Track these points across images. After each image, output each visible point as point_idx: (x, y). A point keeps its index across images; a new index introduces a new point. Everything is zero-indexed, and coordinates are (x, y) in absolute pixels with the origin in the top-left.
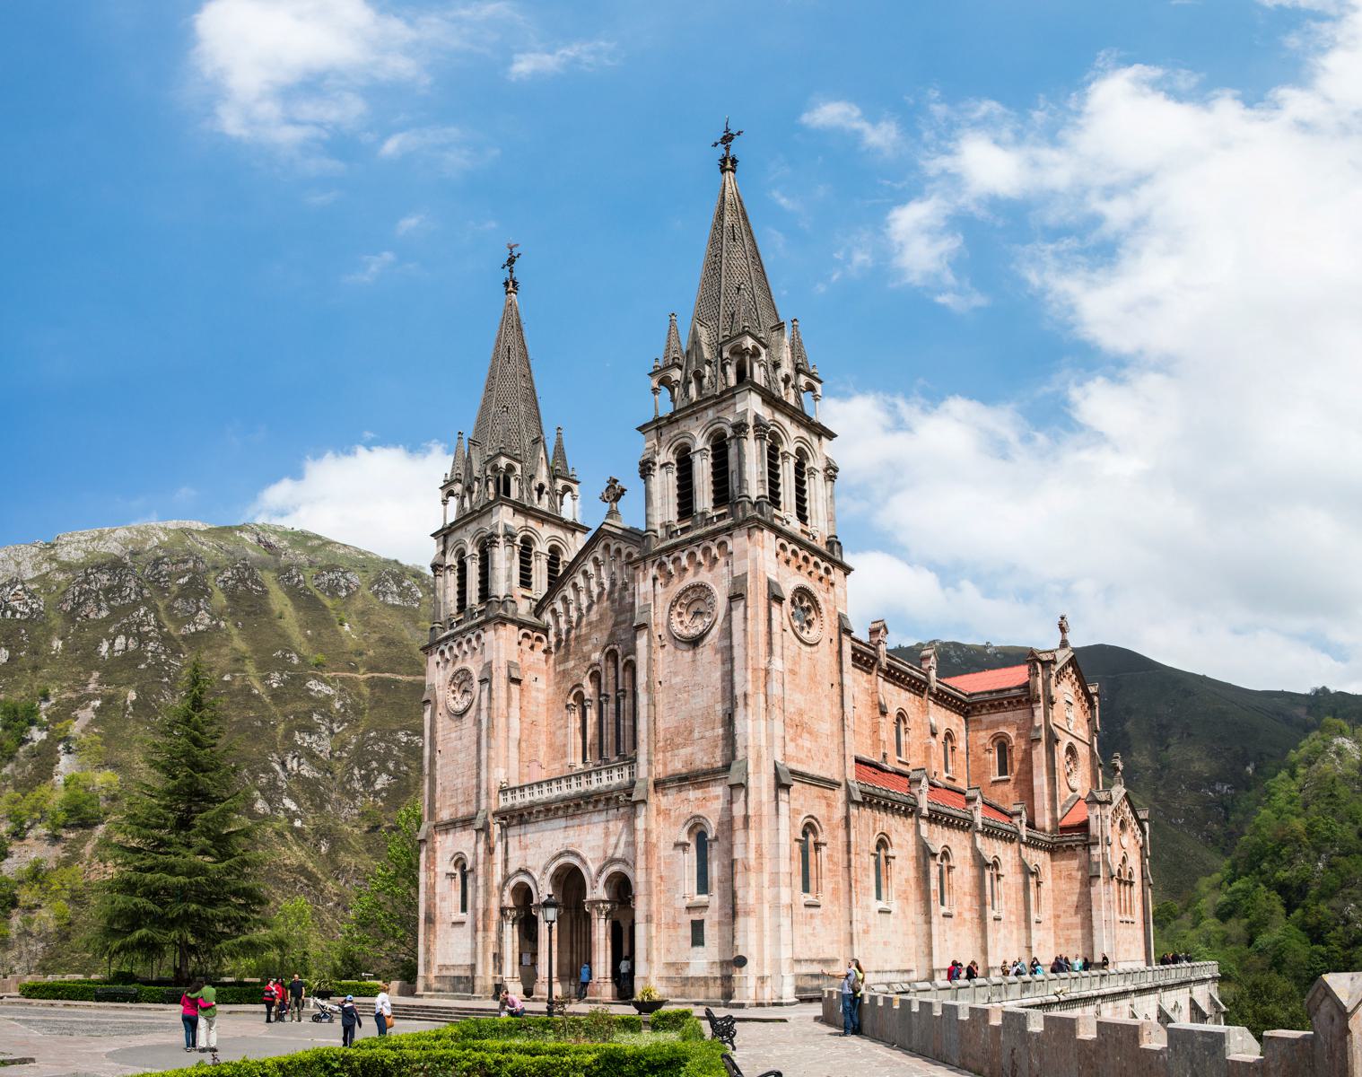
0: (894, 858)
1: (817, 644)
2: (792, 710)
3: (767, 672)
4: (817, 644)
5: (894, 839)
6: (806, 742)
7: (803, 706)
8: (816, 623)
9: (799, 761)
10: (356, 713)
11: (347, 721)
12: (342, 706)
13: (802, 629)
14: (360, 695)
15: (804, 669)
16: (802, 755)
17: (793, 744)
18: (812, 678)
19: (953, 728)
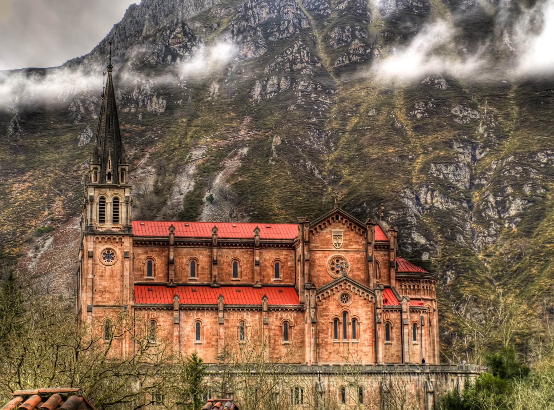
0: (160, 326)
1: (114, 264)
2: (100, 287)
3: (87, 279)
4: (114, 264)
5: (161, 319)
6: (107, 296)
7: (106, 285)
8: (115, 258)
9: (104, 302)
10: (499, 138)
11: (489, 146)
12: (486, 130)
13: (108, 261)
14: (507, 116)
15: (108, 273)
16: (105, 300)
17: (100, 298)
18: (112, 276)
19: (282, 257)
